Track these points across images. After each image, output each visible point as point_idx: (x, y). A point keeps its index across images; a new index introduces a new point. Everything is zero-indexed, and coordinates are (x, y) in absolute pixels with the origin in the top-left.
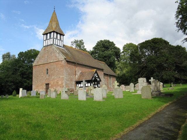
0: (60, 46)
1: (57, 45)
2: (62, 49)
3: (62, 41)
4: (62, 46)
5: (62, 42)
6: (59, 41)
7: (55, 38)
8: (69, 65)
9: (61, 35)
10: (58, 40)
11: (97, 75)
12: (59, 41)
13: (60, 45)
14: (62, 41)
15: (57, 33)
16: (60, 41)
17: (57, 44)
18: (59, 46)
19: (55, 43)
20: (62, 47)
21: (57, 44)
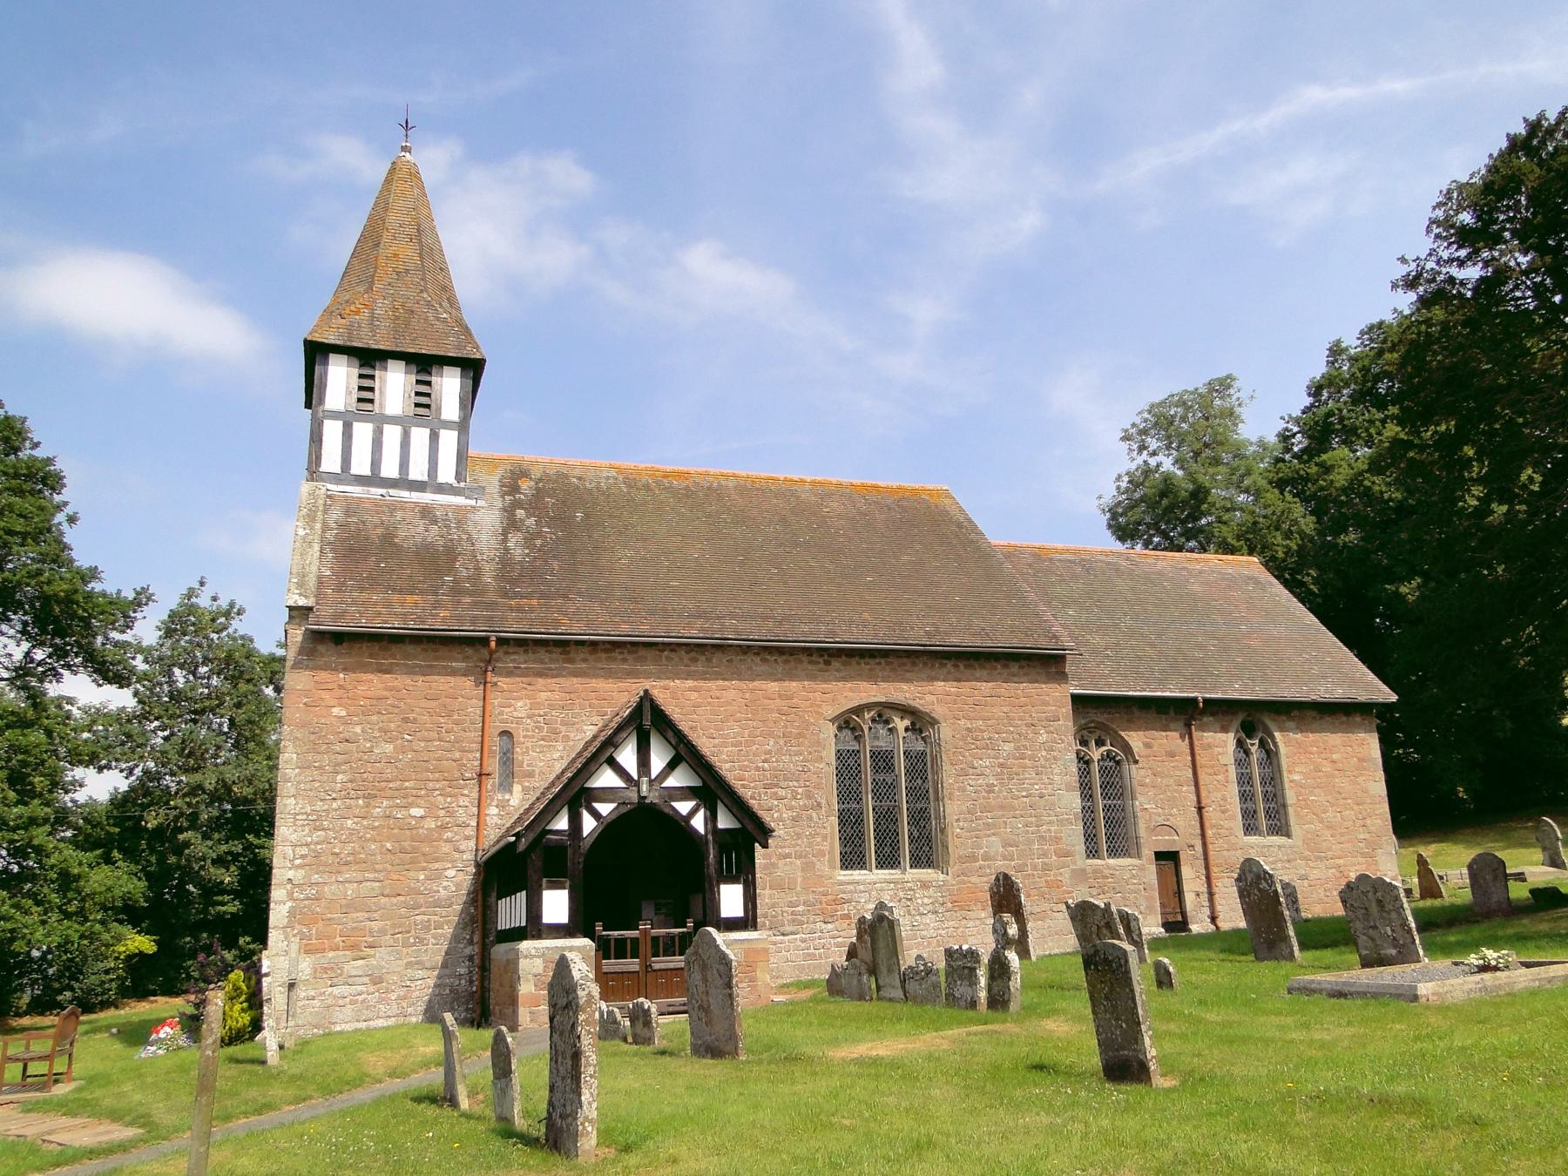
0: (419, 486)
1: (361, 480)
2: (426, 512)
3: (448, 425)
4: (447, 474)
5: (449, 439)
6: (392, 434)
7: (335, 415)
8: (372, 684)
9: (424, 364)
10: (380, 421)
11: (685, 753)
12: (392, 434)
13: (418, 472)
14: (448, 425)
15: (369, 359)
16: (420, 436)
17: (361, 466)
18: (403, 482)
19: (331, 461)
20: (442, 489)
21: (390, 469)
